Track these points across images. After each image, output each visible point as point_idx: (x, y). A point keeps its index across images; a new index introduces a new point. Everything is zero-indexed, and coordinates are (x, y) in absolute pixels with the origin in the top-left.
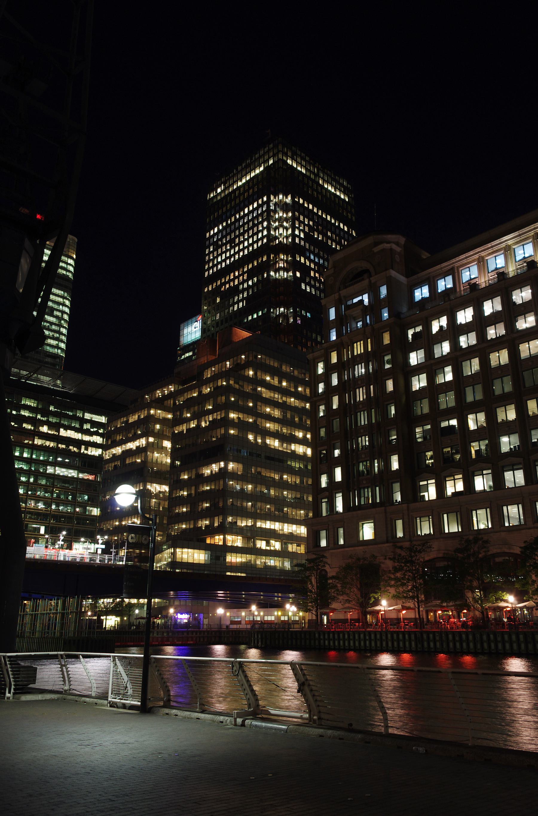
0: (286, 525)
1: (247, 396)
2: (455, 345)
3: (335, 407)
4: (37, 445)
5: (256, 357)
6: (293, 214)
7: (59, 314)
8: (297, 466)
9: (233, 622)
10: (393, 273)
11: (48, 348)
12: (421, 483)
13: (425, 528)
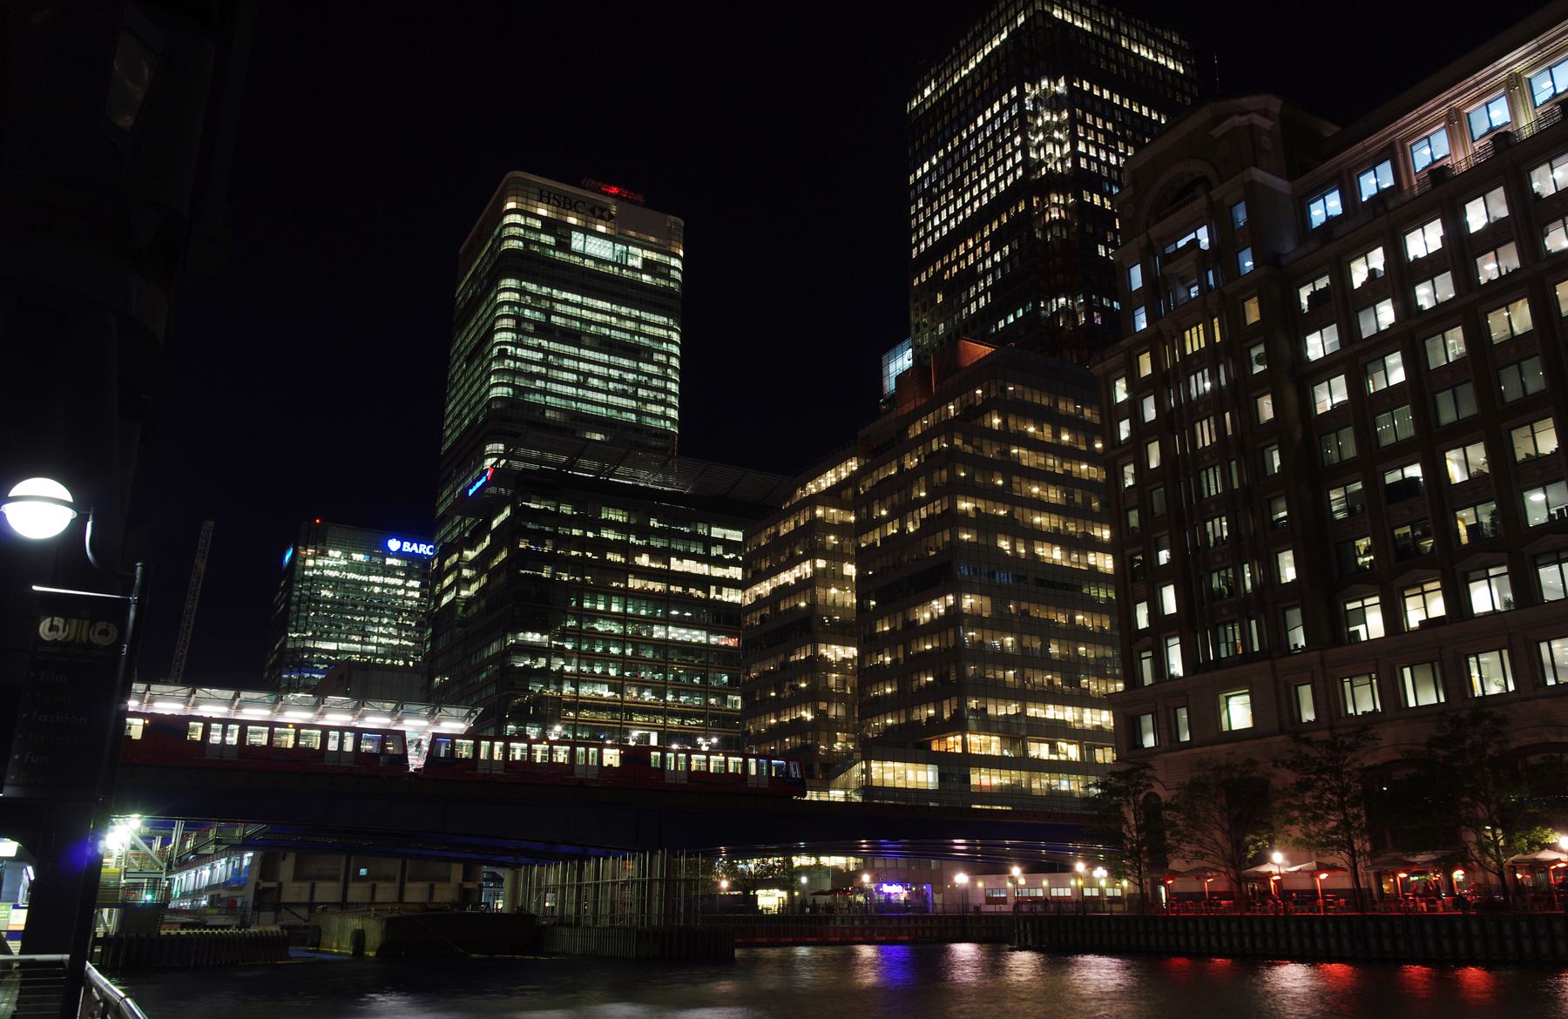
0: (1087, 711)
1: (992, 467)
2: (1406, 306)
3: (1154, 464)
4: (633, 590)
5: (1004, 390)
7: (662, 358)
8: (1103, 595)
9: (990, 900)
10: (1258, 174)
11: (648, 420)
12: (1350, 606)
13: (1364, 700)
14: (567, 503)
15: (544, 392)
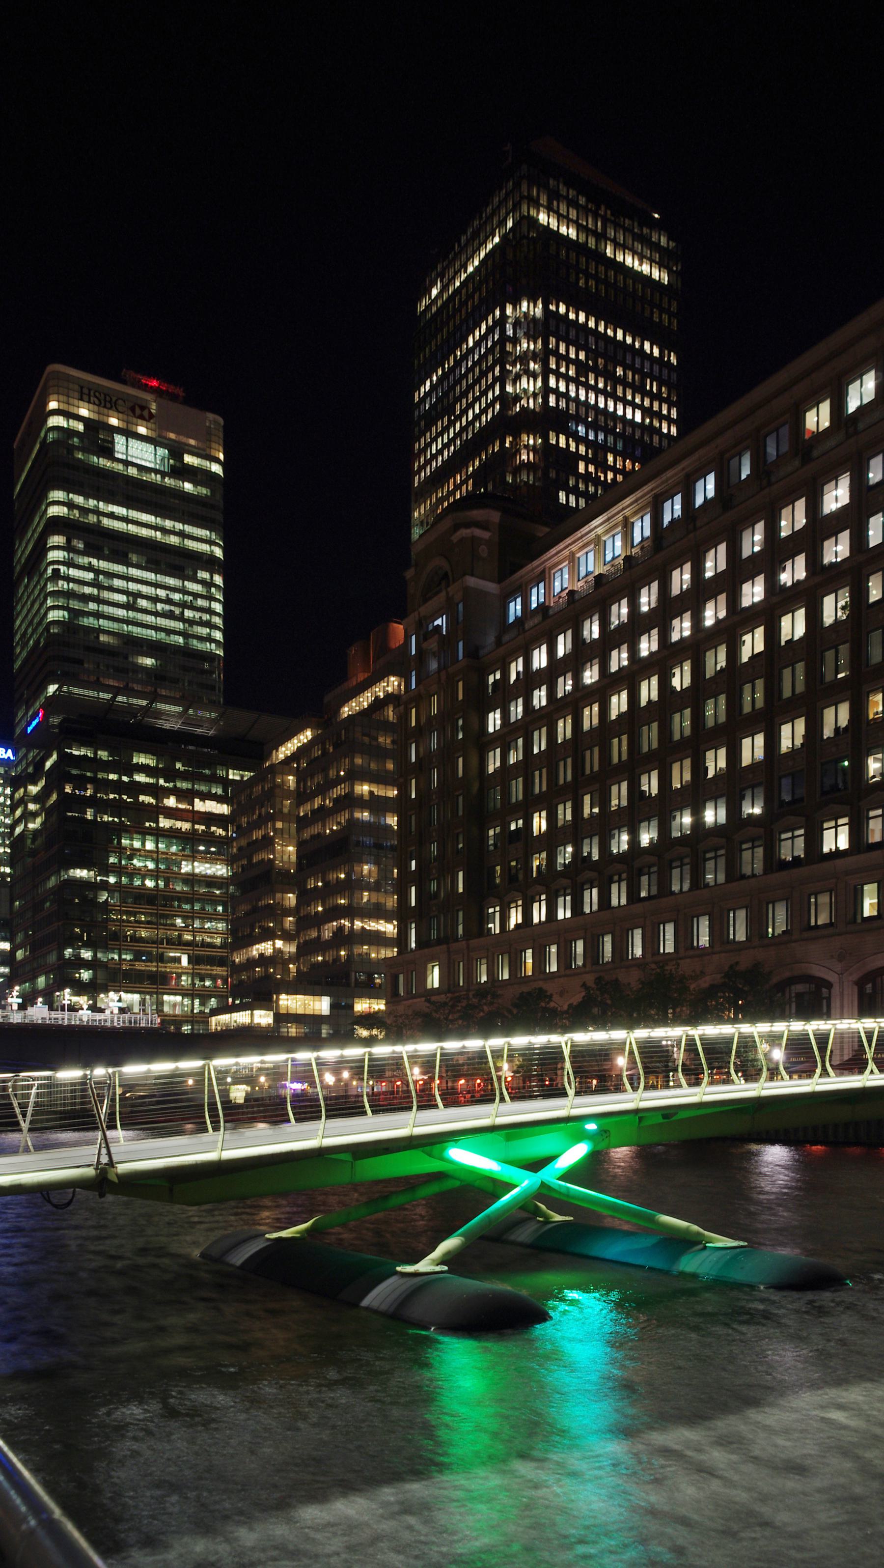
4: (163, 829)
6: (546, 343)
14: (103, 749)
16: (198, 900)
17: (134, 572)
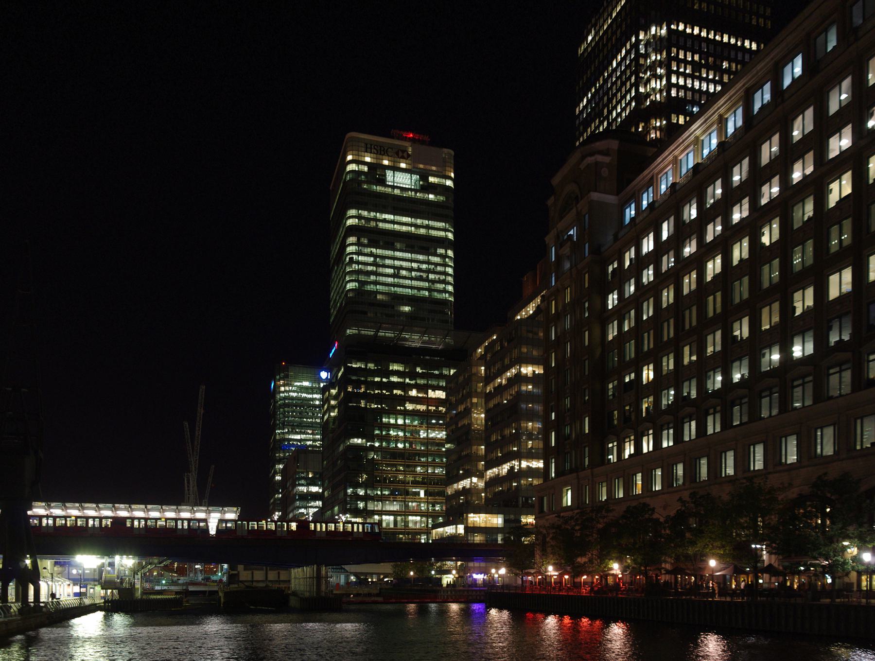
4: (408, 411)
6: (669, 53)
15: (376, 283)
16: (431, 455)
17: (398, 254)
